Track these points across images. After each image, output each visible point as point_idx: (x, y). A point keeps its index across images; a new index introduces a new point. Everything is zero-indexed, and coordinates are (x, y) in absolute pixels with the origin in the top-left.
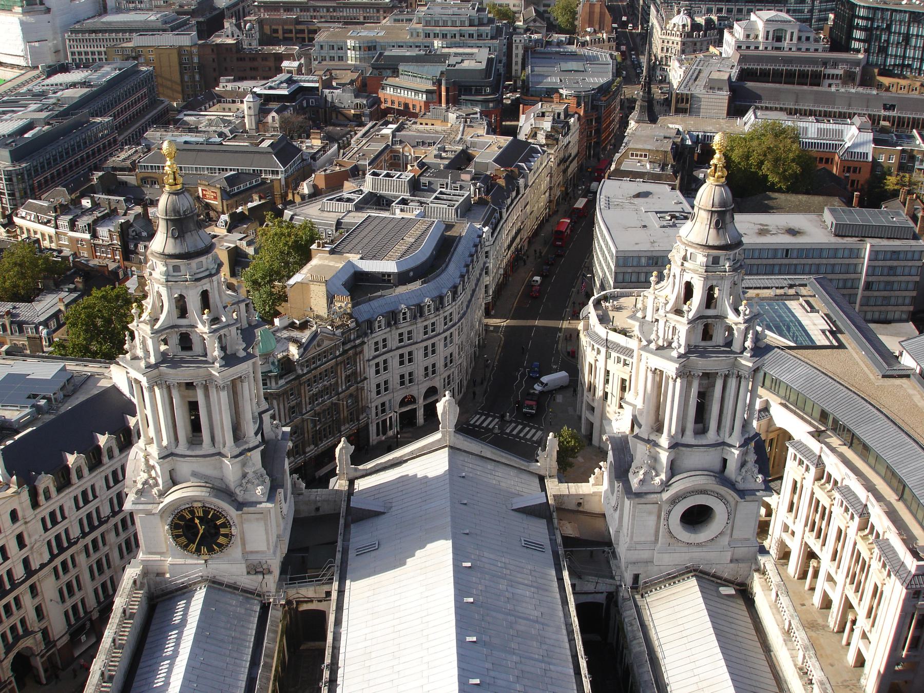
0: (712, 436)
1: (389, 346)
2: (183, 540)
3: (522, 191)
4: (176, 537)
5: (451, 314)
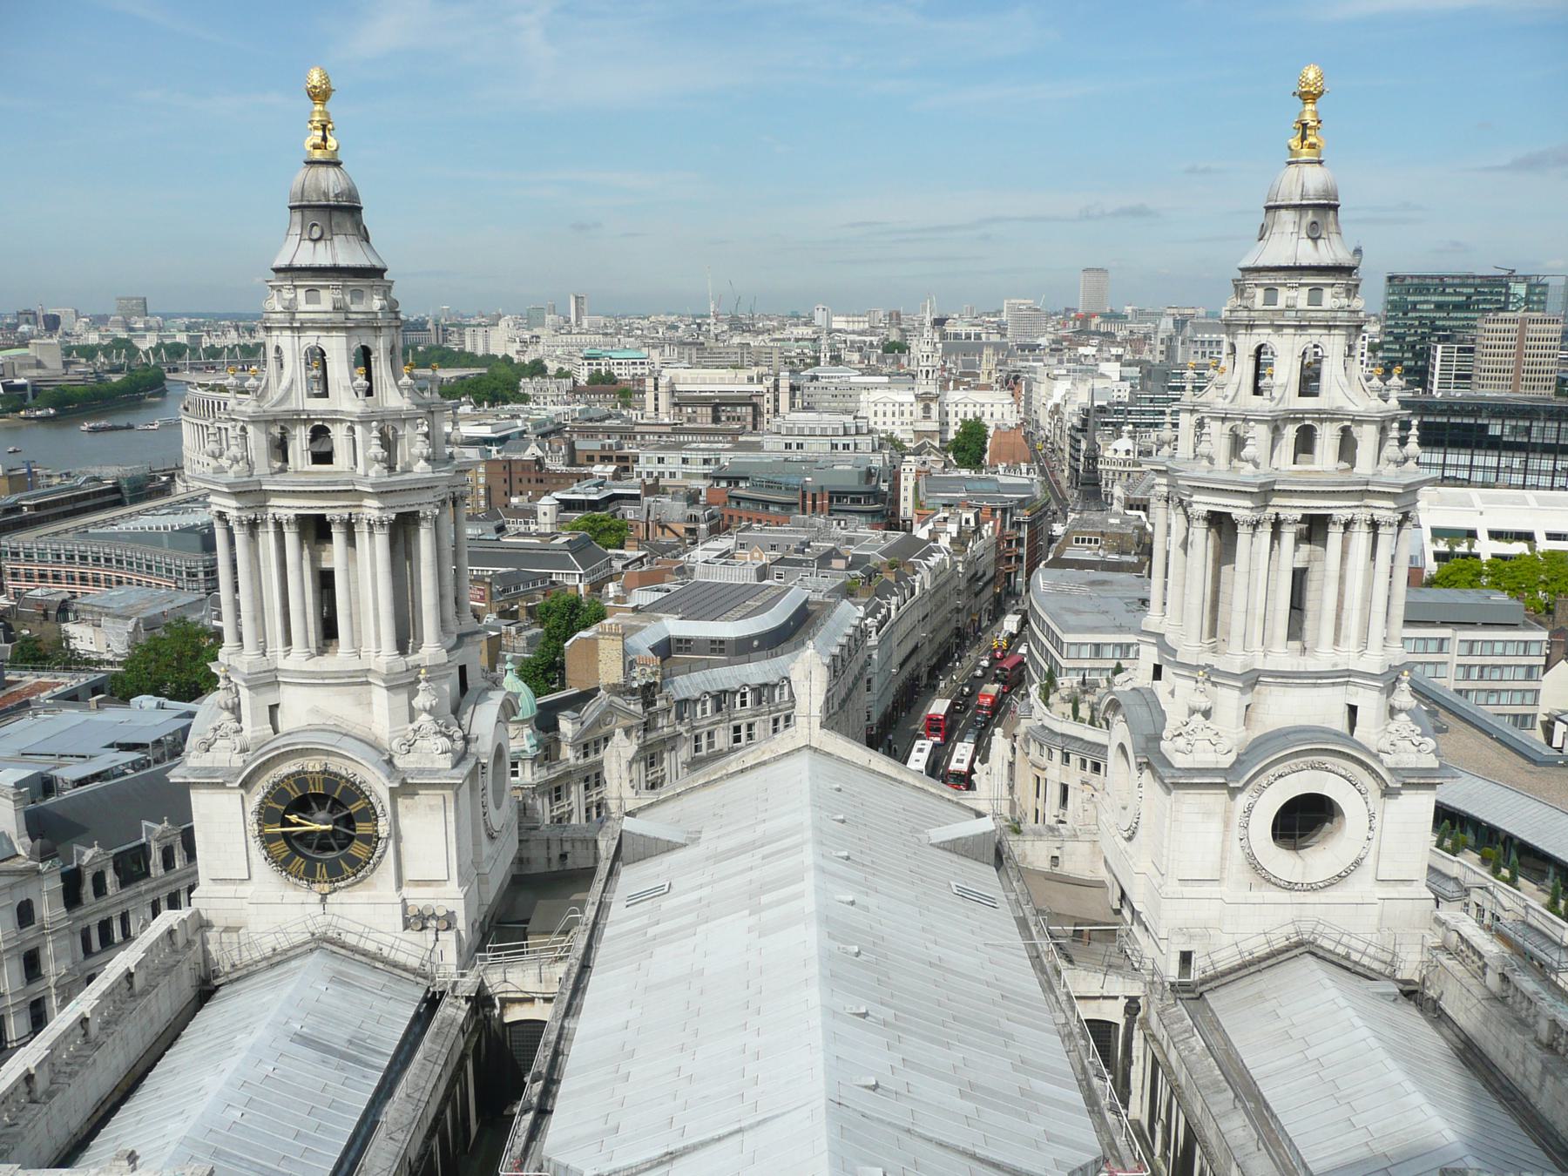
1: (717, 747)
2: (281, 847)
4: (267, 840)
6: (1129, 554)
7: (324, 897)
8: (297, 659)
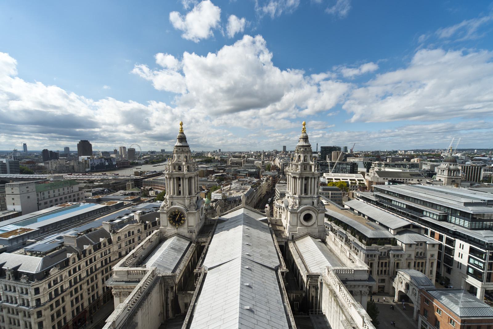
0: (309, 195)
2: (172, 221)
4: (170, 220)
7: (177, 228)
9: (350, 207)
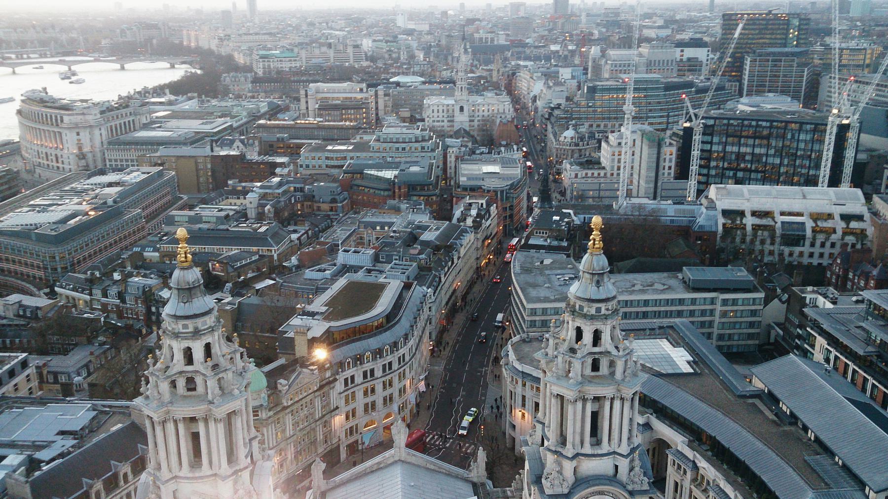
0: (605, 448)
1: (356, 382)
3: (455, 261)
5: (404, 355)
6: (563, 240)
8: (185, 471)
9: (769, 391)
